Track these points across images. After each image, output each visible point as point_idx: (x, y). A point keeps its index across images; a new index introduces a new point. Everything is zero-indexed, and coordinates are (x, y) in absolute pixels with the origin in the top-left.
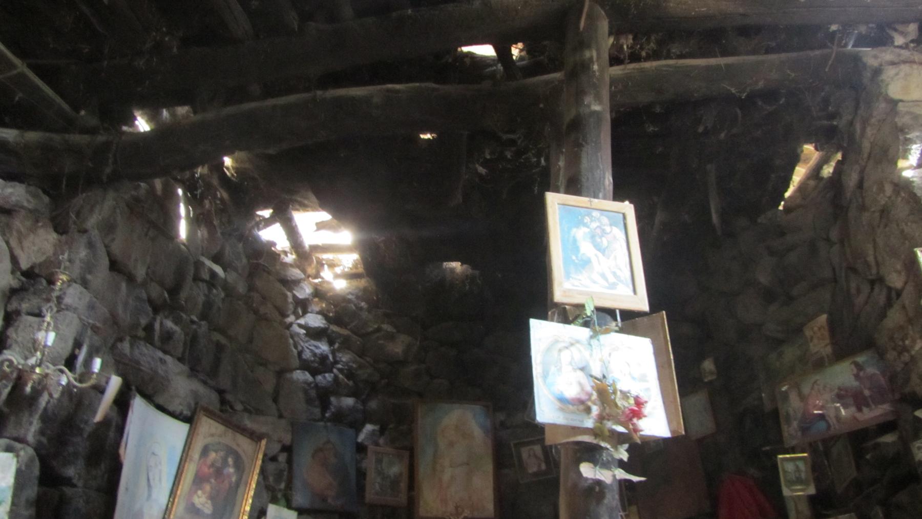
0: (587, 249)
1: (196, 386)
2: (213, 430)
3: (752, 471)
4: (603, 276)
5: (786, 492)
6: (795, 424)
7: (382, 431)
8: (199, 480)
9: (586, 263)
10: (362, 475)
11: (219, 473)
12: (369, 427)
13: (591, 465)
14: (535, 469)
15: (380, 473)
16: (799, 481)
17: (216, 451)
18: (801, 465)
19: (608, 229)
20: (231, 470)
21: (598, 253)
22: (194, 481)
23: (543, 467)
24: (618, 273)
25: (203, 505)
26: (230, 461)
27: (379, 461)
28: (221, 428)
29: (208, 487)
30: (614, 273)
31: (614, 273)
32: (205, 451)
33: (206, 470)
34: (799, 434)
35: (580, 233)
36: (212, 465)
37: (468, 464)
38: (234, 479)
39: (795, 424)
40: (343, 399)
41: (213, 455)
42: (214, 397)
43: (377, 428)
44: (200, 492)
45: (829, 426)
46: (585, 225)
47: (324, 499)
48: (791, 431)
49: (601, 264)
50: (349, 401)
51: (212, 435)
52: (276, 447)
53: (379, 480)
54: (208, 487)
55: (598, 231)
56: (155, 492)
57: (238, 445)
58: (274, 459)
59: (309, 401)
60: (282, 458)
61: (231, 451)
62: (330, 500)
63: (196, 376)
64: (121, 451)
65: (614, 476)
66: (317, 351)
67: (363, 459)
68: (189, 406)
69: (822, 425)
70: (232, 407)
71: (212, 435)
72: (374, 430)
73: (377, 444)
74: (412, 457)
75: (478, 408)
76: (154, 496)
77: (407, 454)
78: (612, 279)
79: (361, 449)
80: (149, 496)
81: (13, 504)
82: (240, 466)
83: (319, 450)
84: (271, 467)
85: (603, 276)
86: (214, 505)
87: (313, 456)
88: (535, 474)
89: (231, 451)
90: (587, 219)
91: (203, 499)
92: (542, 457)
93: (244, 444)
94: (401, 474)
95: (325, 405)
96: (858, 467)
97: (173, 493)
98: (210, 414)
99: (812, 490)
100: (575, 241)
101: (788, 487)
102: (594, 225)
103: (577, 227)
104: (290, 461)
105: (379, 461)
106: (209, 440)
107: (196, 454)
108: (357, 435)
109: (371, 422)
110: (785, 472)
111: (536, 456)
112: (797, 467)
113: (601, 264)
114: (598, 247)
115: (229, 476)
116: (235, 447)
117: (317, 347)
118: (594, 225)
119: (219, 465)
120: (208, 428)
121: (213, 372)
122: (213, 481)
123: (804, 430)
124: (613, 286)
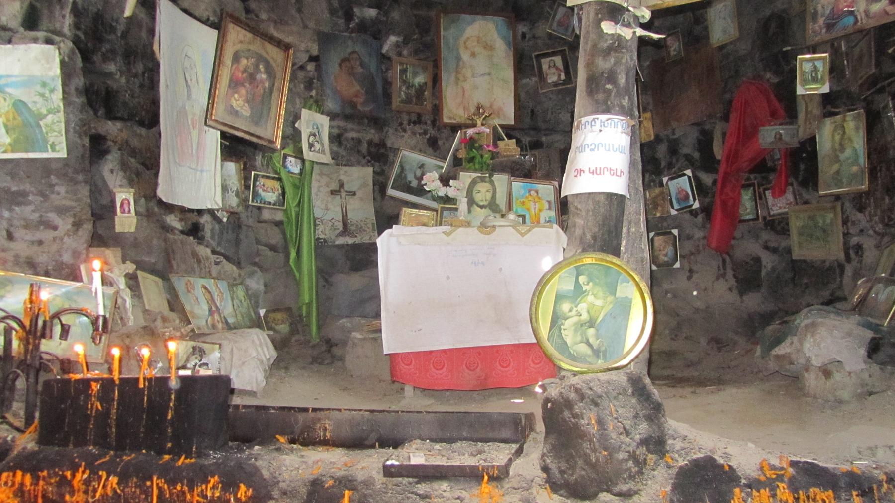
2: (241, 37)
3: (768, 75)
5: (800, 91)
6: (821, 21)
7: (406, 42)
8: (235, 84)
10: (387, 84)
11: (252, 78)
12: (393, 39)
13: (613, 24)
14: (555, 79)
15: (404, 82)
16: (815, 80)
17: (247, 59)
18: (819, 65)
20: (264, 76)
22: (230, 86)
23: (563, 77)
25: (241, 107)
27: (404, 71)
28: (249, 35)
29: (243, 91)
32: (236, 58)
34: (824, 31)
36: (245, 71)
37: (489, 74)
38: (267, 85)
39: (821, 21)
40: (366, 10)
41: (244, 61)
43: (400, 39)
44: (236, 96)
45: (856, 21)
47: (353, 106)
48: (816, 29)
50: (372, 13)
51: (241, 42)
52: (304, 57)
53: (404, 89)
56: (194, 91)
57: (267, 53)
58: (302, 67)
59: (333, 12)
60: (311, 67)
61: (260, 58)
62: (359, 107)
64: (156, 47)
65: (635, 33)
67: (387, 69)
68: (215, 12)
69: (850, 20)
70: (257, 16)
71: (241, 42)
72: (397, 41)
73: (400, 54)
74: (436, 65)
75: (499, 20)
76: (194, 96)
77: (430, 65)
79: (385, 58)
80: (189, 96)
81: (64, 92)
83: (344, 60)
84: (301, 75)
86: (251, 108)
87: (340, 65)
88: (556, 85)
89: (260, 58)
91: (241, 102)
92: (562, 67)
93: (274, 54)
94: (426, 83)
95: (348, 16)
96: (878, 64)
97: (211, 95)
98: (237, 21)
99: (826, 89)
101: (803, 86)
104: (318, 68)
105: (404, 71)
106: (238, 47)
108: (381, 47)
109: (394, 34)
110: (803, 73)
112: (815, 67)
115: (262, 82)
116: (264, 54)
119: (251, 70)
120: (236, 35)
122: (247, 85)
123: (830, 27)
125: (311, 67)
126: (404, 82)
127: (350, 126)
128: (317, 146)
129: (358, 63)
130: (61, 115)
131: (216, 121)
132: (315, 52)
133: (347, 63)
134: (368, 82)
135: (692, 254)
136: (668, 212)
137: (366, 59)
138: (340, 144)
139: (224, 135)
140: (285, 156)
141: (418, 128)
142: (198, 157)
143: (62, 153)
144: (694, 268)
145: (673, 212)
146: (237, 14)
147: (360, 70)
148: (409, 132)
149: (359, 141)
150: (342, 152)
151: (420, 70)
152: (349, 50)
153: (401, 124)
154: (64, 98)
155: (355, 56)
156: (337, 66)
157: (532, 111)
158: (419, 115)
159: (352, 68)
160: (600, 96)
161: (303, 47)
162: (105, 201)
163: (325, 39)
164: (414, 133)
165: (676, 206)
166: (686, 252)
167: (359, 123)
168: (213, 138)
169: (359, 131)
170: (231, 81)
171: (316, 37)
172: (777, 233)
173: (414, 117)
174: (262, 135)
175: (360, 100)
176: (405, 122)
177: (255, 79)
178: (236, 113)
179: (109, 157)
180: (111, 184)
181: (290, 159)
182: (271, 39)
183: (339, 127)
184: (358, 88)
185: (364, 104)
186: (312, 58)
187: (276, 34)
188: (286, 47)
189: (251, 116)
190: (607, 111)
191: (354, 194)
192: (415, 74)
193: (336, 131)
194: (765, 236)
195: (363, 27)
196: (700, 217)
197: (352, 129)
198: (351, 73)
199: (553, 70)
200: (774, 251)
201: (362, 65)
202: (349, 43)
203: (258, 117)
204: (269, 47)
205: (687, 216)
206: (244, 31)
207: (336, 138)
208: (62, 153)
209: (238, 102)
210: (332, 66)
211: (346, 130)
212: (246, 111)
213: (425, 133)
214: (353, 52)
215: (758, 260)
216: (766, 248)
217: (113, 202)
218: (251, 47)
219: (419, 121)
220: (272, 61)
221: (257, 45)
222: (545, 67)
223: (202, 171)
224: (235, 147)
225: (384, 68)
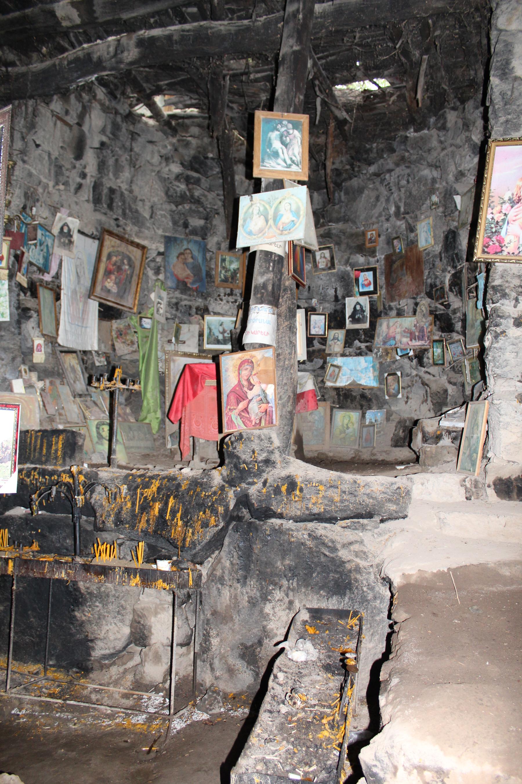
0: (277, 145)
1: (99, 216)
2: (113, 243)
4: (285, 161)
9: (276, 154)
11: (119, 269)
19: (291, 131)
20: (127, 267)
21: (284, 147)
22: (105, 274)
23: (329, 265)
24: (294, 158)
26: (125, 261)
28: (118, 242)
29: (113, 277)
30: (291, 159)
31: (291, 159)
32: (109, 257)
33: (111, 267)
35: (274, 135)
36: (115, 264)
38: (129, 272)
41: (114, 259)
42: (113, 223)
46: (278, 130)
47: (185, 284)
49: (285, 154)
50: (202, 222)
51: (113, 247)
54: (113, 277)
55: (285, 133)
58: (153, 260)
61: (125, 256)
62: (189, 285)
63: (99, 211)
66: (178, 189)
67: (211, 259)
68: (97, 229)
70: (124, 229)
73: (219, 249)
76: (82, 282)
78: (289, 162)
82: (131, 264)
83: (181, 254)
84: (152, 264)
85: (285, 161)
86: (118, 287)
87: (178, 257)
88: (323, 270)
90: (279, 126)
91: (111, 284)
92: (329, 258)
95: (186, 225)
98: (111, 233)
100: (270, 139)
102: (283, 129)
103: (272, 131)
104: (164, 260)
106: (111, 249)
107: (104, 258)
111: (324, 257)
113: (285, 154)
114: (283, 143)
115: (125, 271)
117: (178, 187)
118: (283, 129)
119: (118, 264)
120: (110, 242)
121: (110, 207)
124: (289, 166)
125: (159, 259)
126: (224, 268)
127: (184, 297)
128: (161, 311)
129: (190, 256)
130: (7, 298)
131: (96, 296)
132: (162, 250)
133: (183, 257)
134: (196, 269)
135: (409, 386)
136: (395, 358)
137: (196, 253)
138: (177, 309)
139: (101, 305)
140: (141, 318)
141: (231, 299)
142: (83, 319)
143: (7, 319)
144: (410, 396)
145: (398, 358)
146: (111, 229)
147: (190, 260)
148: (225, 301)
149: (190, 307)
150: (179, 315)
151: (233, 259)
152: (185, 247)
153: (219, 296)
154: (9, 289)
155: (188, 251)
156: (175, 259)
157: (309, 287)
158: (232, 290)
159: (186, 259)
160: (259, 296)
161: (154, 246)
162: (29, 345)
163: (169, 241)
164: (228, 302)
165: (400, 354)
166: (405, 385)
167: (190, 295)
168: (94, 306)
169: (190, 301)
170: (106, 271)
171: (163, 240)
172: (455, 372)
173: (228, 291)
174: (125, 304)
175: (189, 281)
176: (222, 295)
177: (121, 269)
178: (109, 291)
179: (32, 320)
180: (32, 335)
181: (144, 319)
182: (132, 243)
183: (177, 298)
184: (189, 272)
185: (194, 282)
186: (160, 254)
187: (137, 240)
188: (143, 248)
189: (118, 292)
190: (261, 303)
191: (184, 343)
192: (231, 262)
193: (174, 301)
194: (452, 374)
195: (194, 232)
196: (415, 361)
197: (185, 299)
198: (185, 263)
199: (324, 260)
200: (455, 384)
201: (192, 258)
202: (185, 243)
203: (123, 291)
204: (131, 248)
205: (406, 360)
206: (114, 240)
207: (175, 305)
208: (7, 319)
209: (110, 284)
210: (173, 259)
211: (181, 300)
212: (114, 289)
213: (236, 301)
214: (186, 249)
215: (446, 391)
216: (450, 383)
217: (33, 345)
218: (119, 249)
219: (231, 294)
220: (133, 258)
221: (123, 248)
222: (318, 258)
223: (86, 327)
224: (108, 313)
225: (208, 258)
